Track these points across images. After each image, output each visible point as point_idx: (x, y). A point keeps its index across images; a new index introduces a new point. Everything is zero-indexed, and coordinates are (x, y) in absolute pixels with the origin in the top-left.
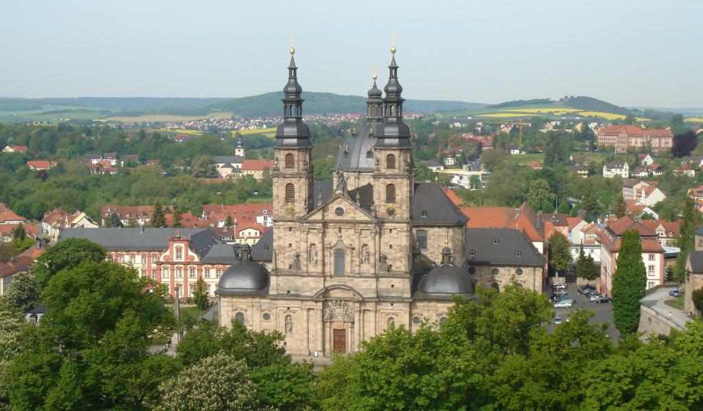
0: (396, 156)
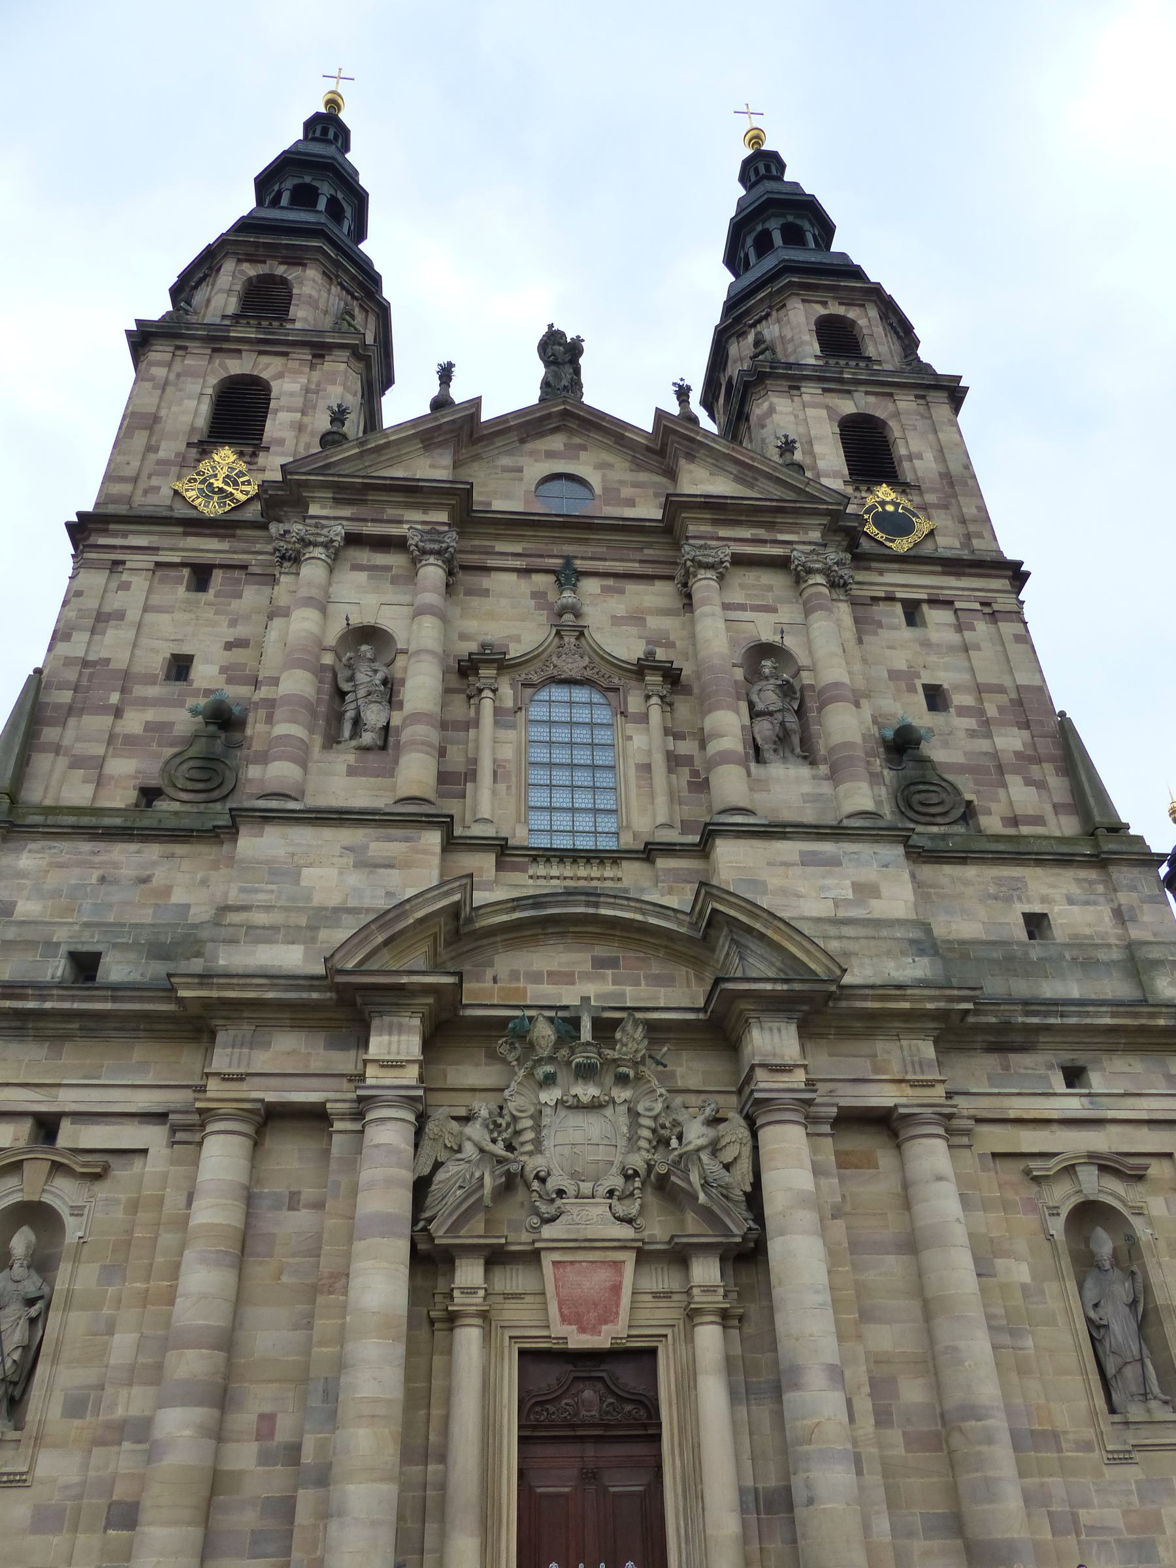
0: (862, 322)
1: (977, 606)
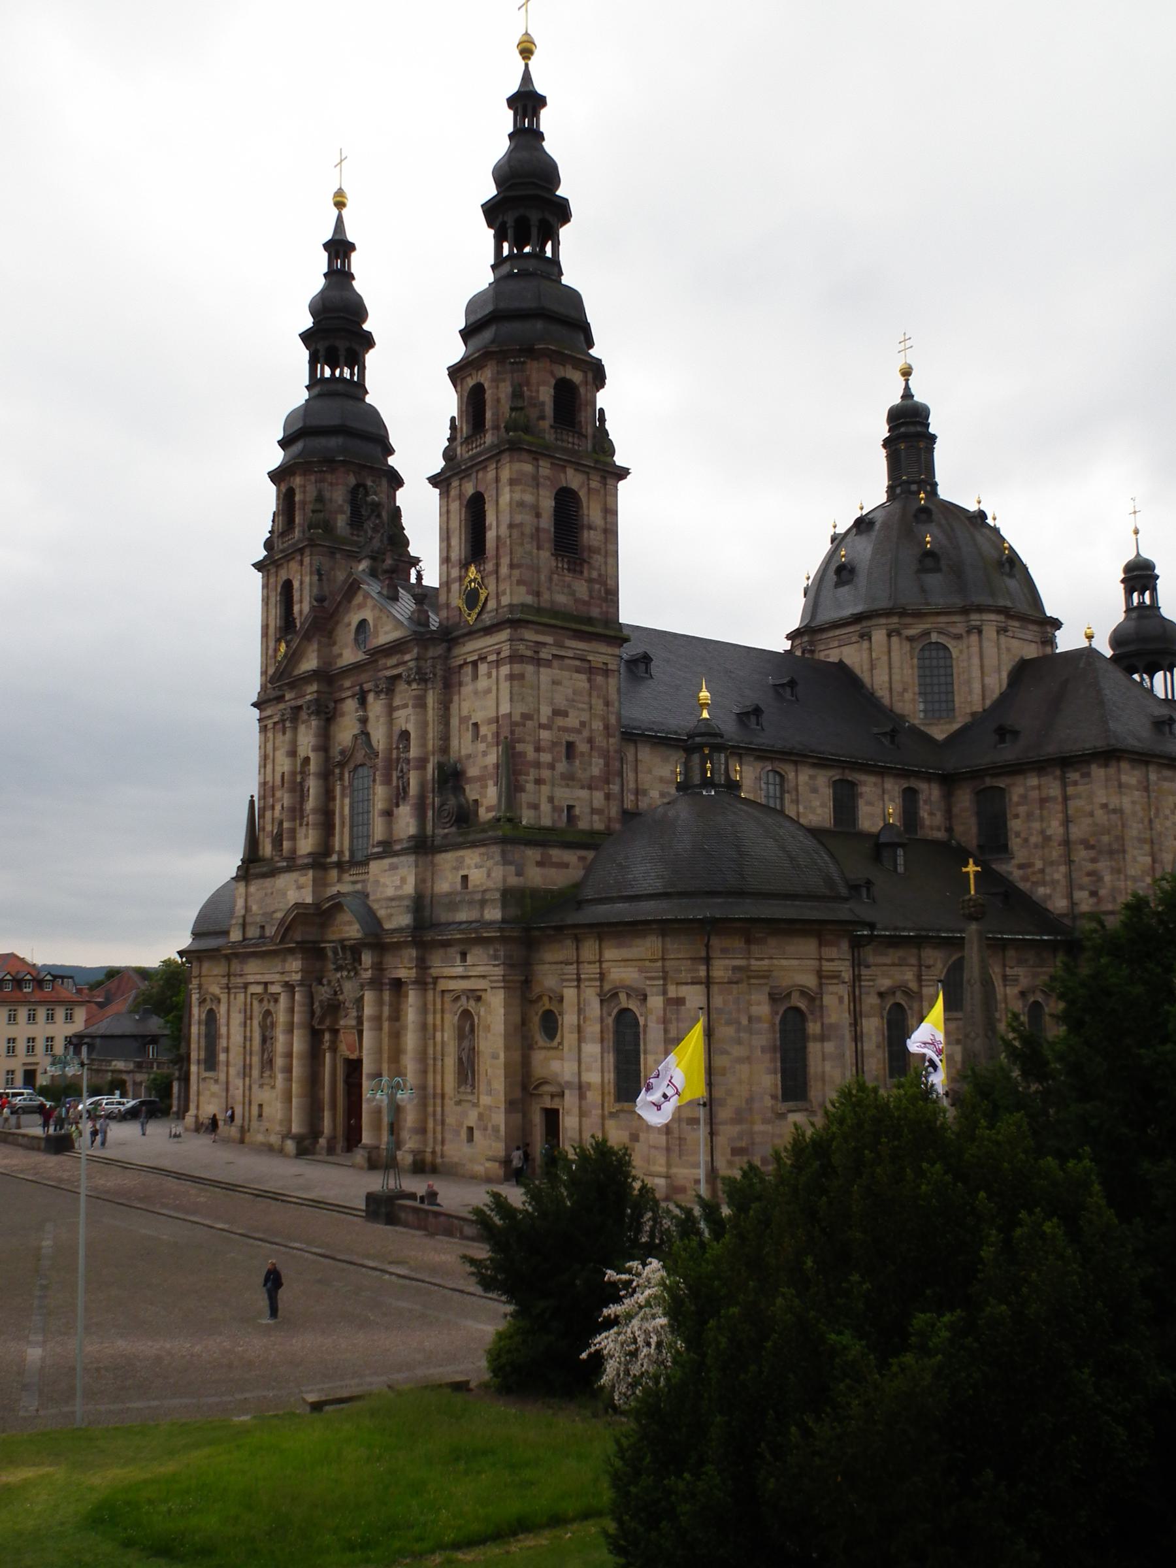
0: (486, 386)
1: (493, 658)
